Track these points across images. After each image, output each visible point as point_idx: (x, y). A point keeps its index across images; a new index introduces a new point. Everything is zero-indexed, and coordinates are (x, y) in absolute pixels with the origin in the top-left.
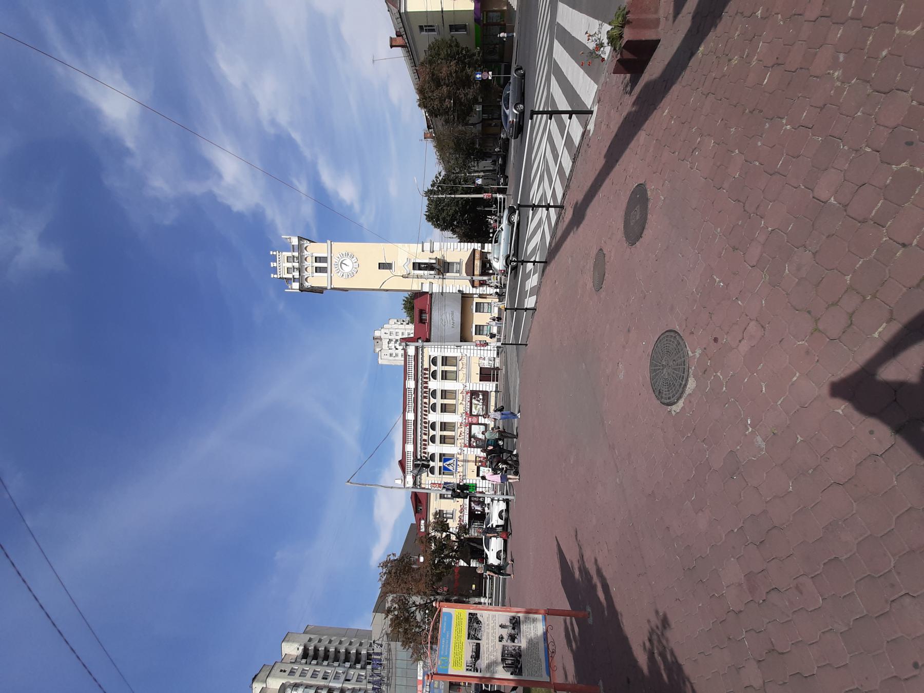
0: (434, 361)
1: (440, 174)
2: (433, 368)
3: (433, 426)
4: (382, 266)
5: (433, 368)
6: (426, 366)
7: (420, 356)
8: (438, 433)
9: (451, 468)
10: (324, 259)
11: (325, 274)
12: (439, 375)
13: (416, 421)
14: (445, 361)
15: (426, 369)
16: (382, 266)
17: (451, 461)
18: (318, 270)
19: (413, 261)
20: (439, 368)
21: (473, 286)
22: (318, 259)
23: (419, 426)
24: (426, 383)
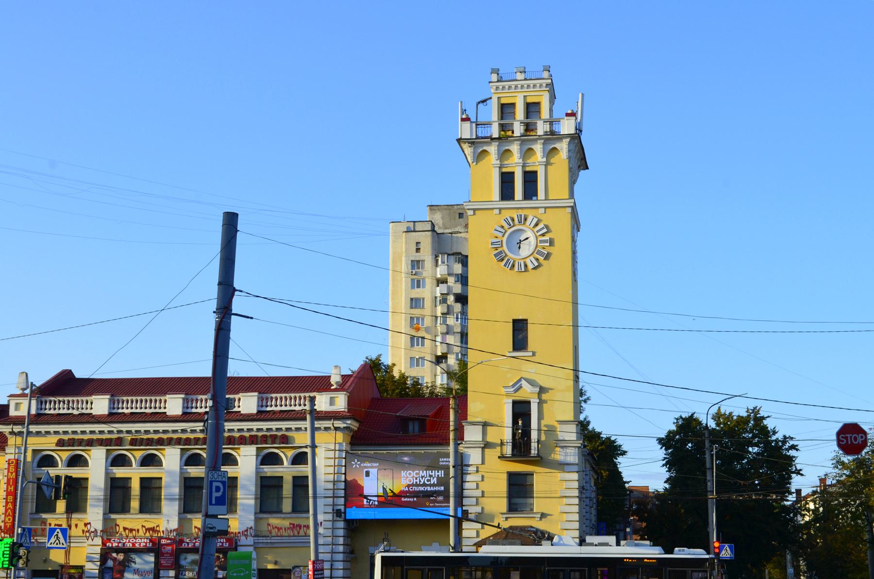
1: (793, 447)
2: (287, 456)
3: (150, 461)
4: (520, 327)
5: (287, 456)
8: (134, 474)
9: (53, 540)
10: (530, 192)
11: (496, 194)
12: (270, 470)
13: (162, 418)
15: (285, 439)
16: (520, 327)
17: (62, 540)
18: (507, 180)
22: (530, 178)
23: (151, 427)
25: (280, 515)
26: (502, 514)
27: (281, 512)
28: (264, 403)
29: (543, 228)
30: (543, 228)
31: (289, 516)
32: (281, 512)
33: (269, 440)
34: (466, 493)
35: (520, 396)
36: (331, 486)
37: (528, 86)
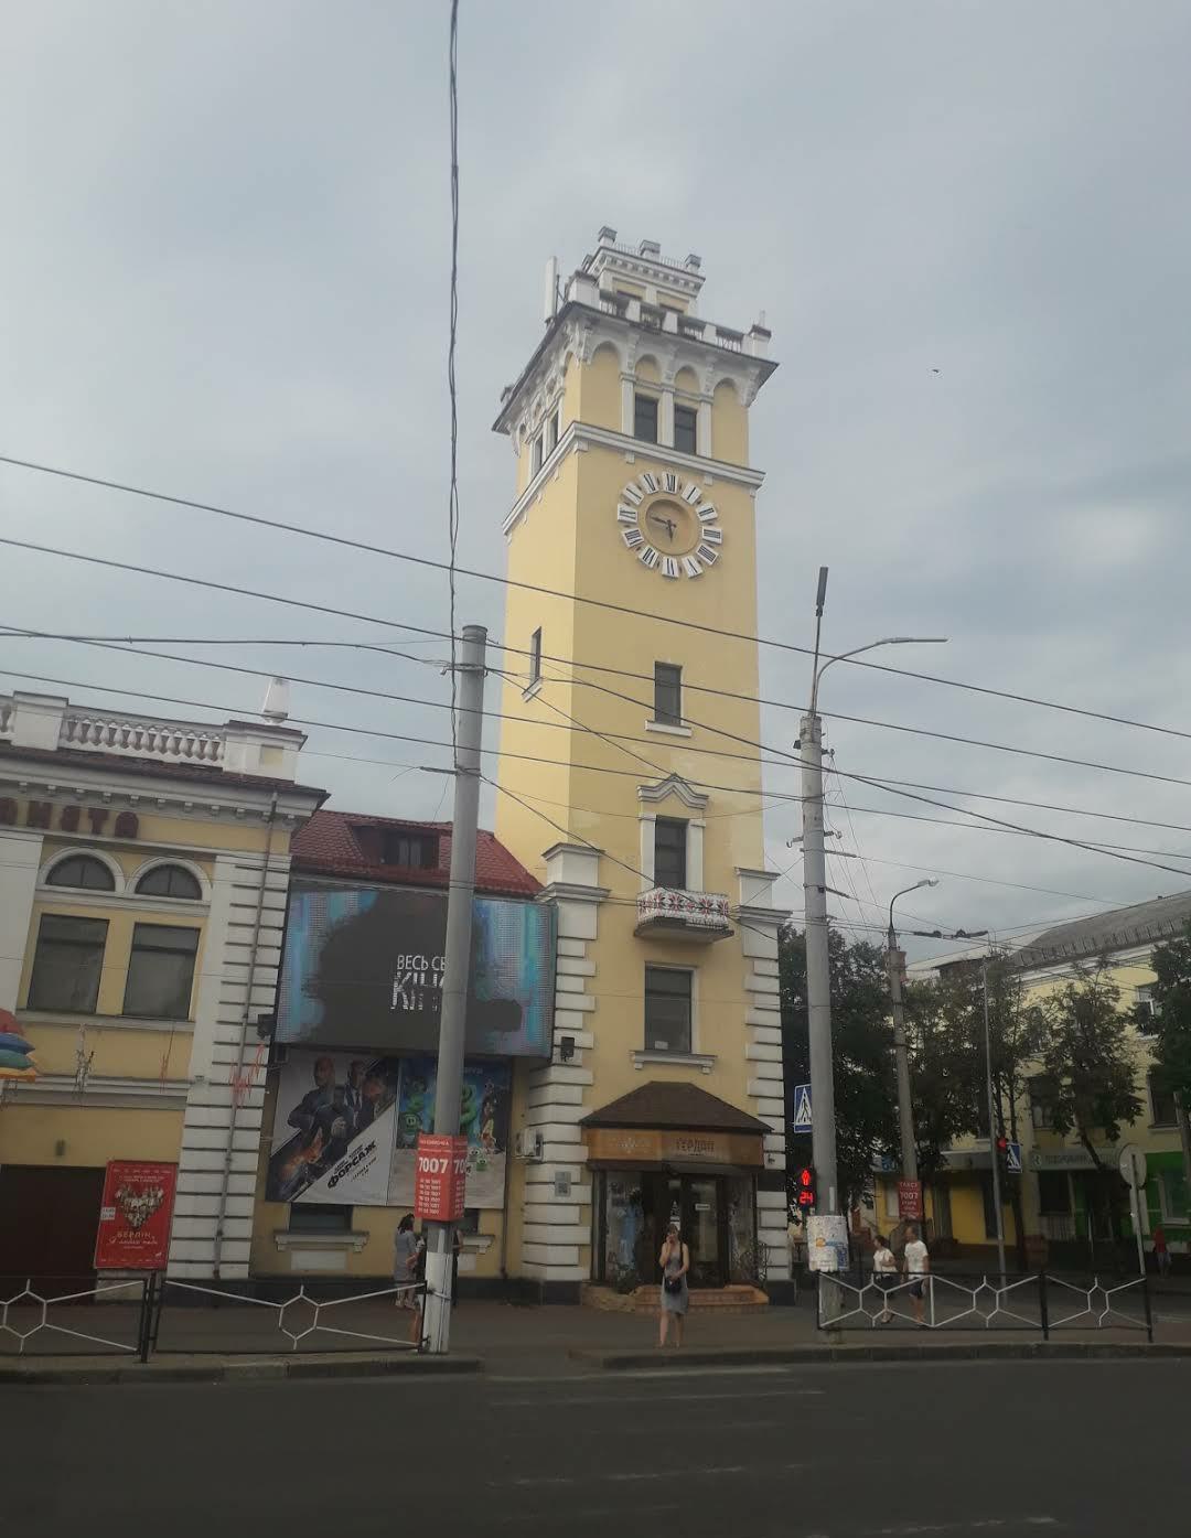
0: (174, 878)
6: (159, 831)
7: (217, 798)
12: (74, 902)
14: (169, 953)
15: (128, 826)
18: (646, 410)
19: (695, 819)
20: (122, 911)
21: (589, 1124)
22: (686, 421)
24: (38, 818)
25: (90, 1021)
26: (637, 1053)
27: (92, 1013)
28: (78, 731)
29: (710, 510)
30: (710, 510)
31: (116, 1023)
32: (92, 1013)
33: (85, 824)
34: (562, 1000)
35: (673, 809)
36: (243, 955)
37: (666, 277)
